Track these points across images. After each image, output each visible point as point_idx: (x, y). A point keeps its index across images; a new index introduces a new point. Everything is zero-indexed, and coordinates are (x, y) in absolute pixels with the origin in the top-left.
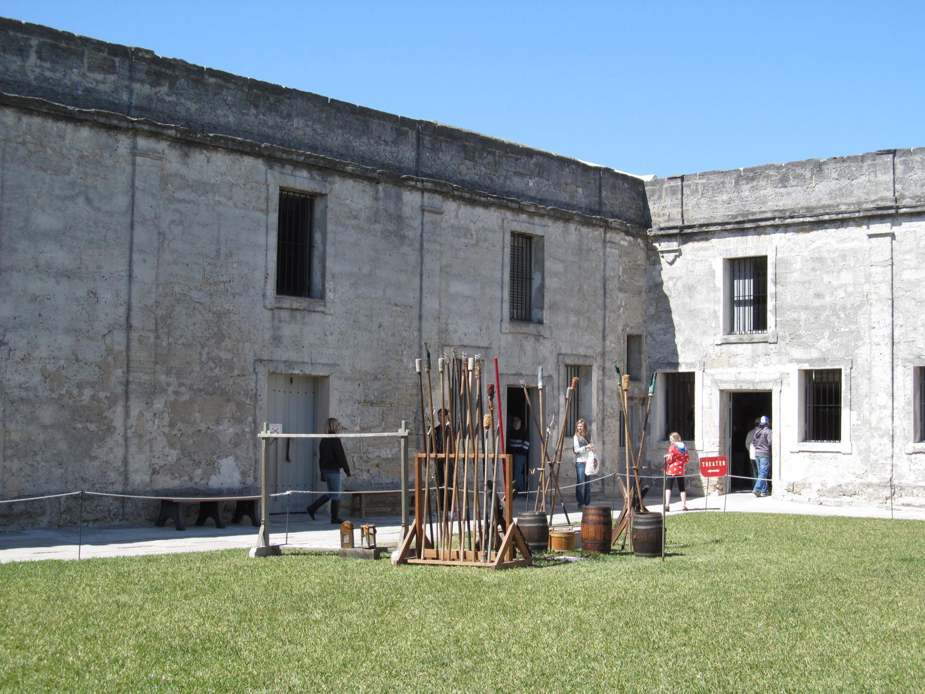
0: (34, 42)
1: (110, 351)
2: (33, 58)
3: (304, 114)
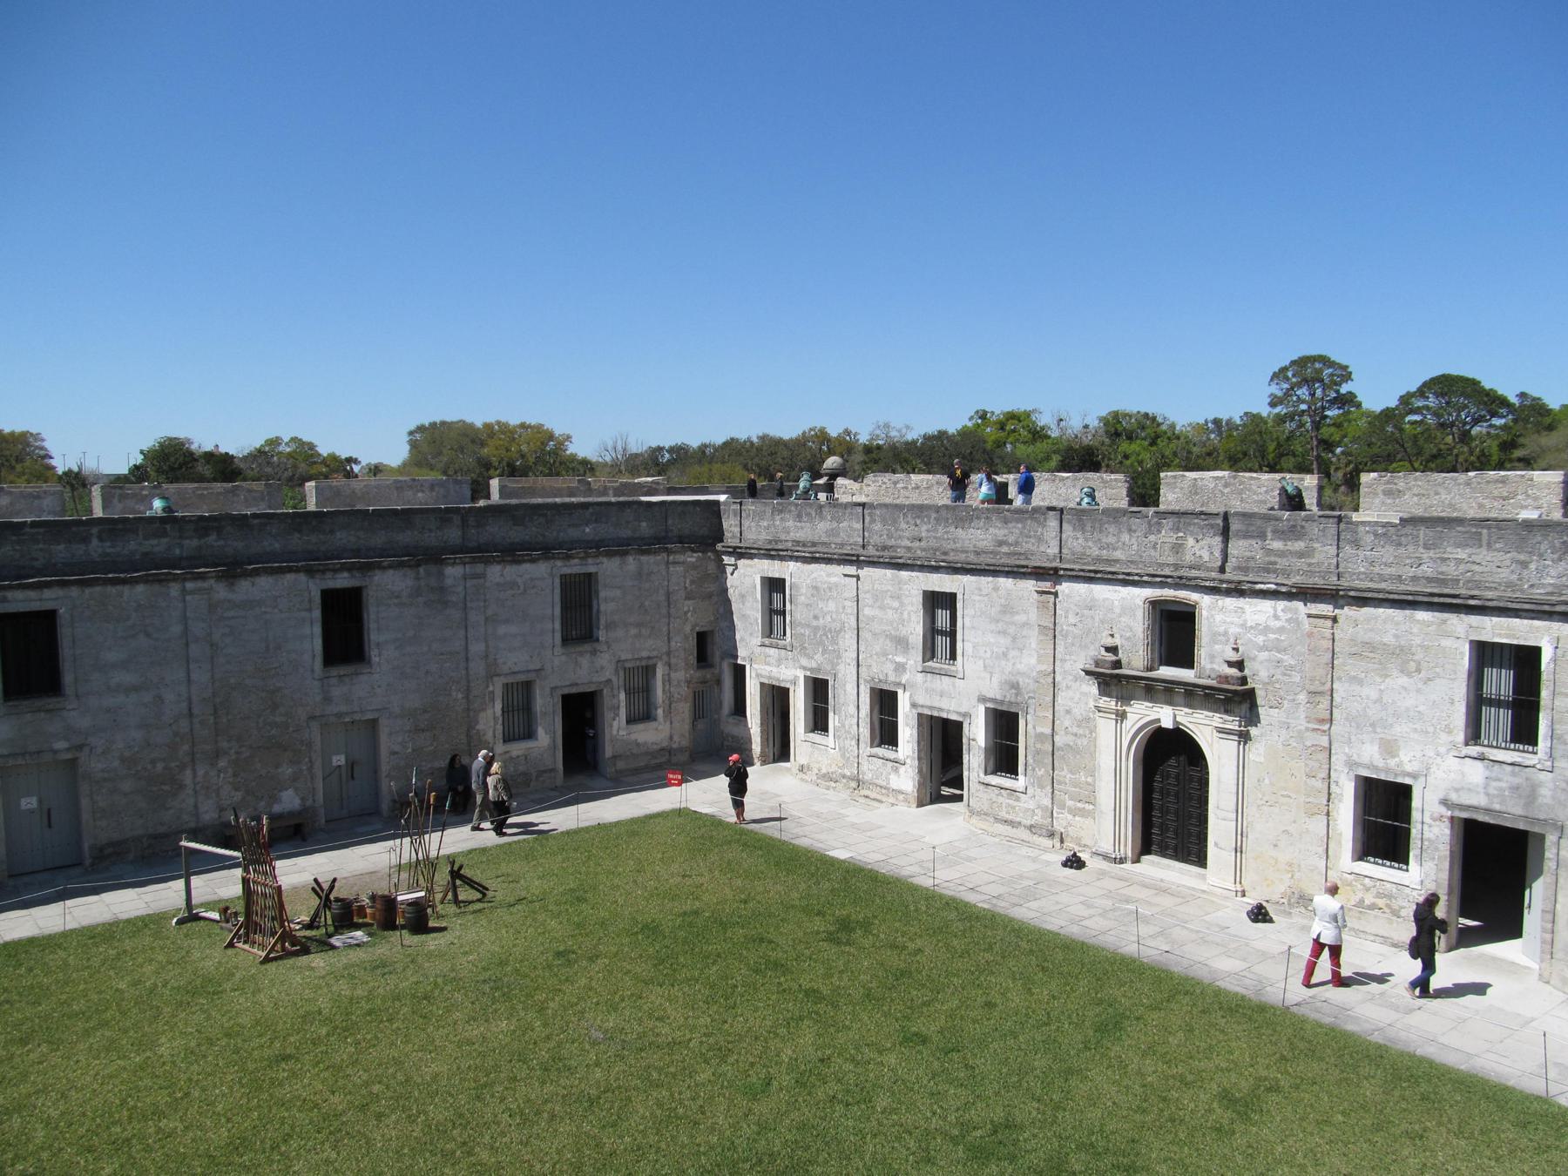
0: (95, 531)
1: (176, 734)
2: (95, 542)
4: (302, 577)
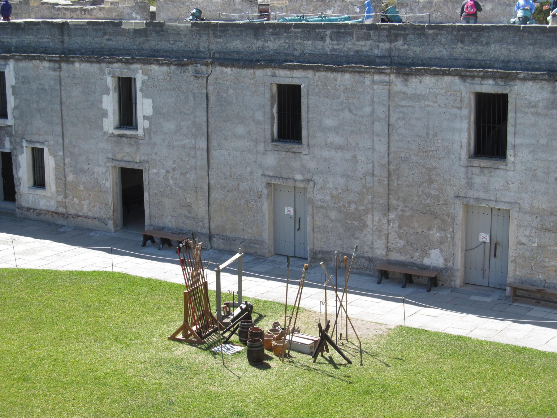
0: (328, 32)
1: (364, 186)
2: (328, 40)
3: (500, 41)
4: (456, 80)
